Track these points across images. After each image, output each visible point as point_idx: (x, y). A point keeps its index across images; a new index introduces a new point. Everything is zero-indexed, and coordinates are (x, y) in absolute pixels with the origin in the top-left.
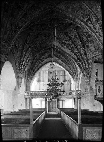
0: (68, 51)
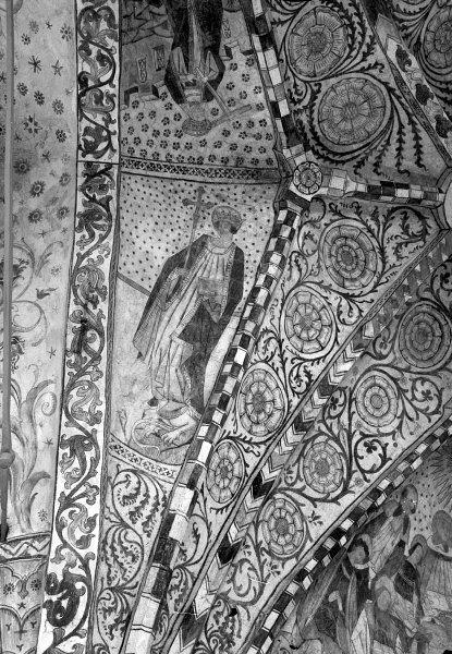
0: (130, 396)
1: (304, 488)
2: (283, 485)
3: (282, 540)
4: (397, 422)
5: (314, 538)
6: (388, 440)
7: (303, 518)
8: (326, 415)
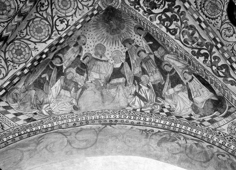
1: (30, 38)
2: (19, 37)
3: (19, 57)
4: (74, 11)
5: (34, 55)
6: (70, 18)
7: (30, 49)
8: (39, 10)
